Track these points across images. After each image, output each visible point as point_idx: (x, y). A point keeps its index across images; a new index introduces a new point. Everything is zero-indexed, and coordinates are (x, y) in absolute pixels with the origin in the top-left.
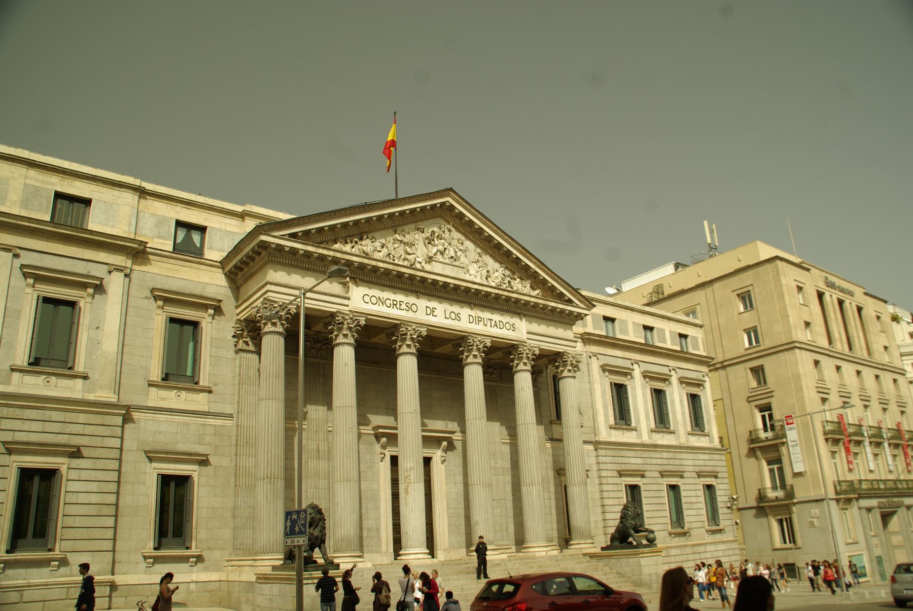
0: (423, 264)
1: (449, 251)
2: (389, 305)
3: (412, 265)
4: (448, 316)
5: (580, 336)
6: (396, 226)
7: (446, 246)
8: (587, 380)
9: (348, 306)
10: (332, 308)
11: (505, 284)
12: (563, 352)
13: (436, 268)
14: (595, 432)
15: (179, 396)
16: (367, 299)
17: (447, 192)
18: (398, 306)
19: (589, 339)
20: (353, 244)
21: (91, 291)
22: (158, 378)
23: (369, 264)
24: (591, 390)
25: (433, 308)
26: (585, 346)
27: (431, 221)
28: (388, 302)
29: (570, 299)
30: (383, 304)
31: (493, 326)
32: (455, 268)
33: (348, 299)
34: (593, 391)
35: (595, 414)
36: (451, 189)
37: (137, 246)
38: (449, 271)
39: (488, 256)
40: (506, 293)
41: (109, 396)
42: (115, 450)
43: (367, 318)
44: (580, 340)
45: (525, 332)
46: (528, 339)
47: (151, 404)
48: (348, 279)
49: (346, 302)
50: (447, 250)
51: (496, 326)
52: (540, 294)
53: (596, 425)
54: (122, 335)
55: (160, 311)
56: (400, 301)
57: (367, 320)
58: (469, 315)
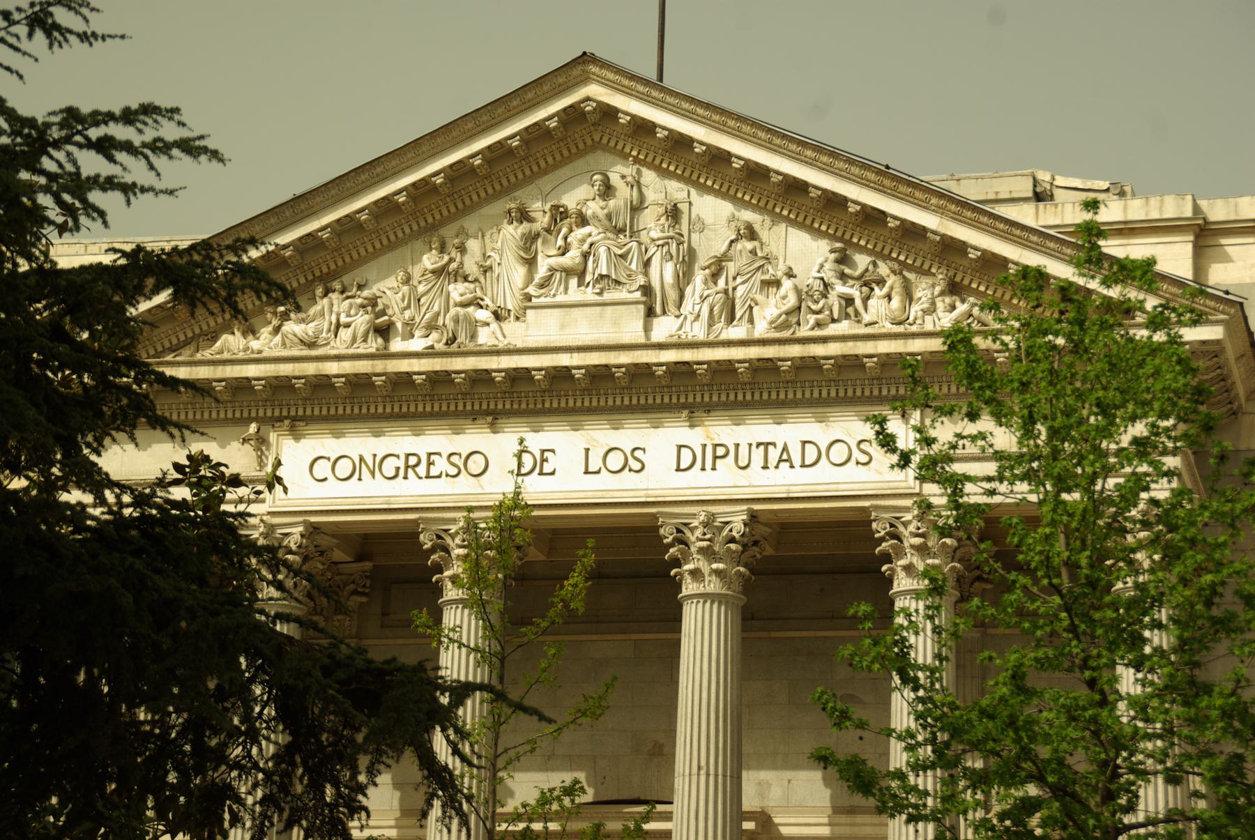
0: (494, 326)
1: (596, 261)
2: (392, 474)
3: (453, 339)
6: (432, 228)
7: (586, 247)
17: (576, 72)
18: (422, 470)
23: (297, 373)
25: (543, 451)
27: (564, 172)
28: (389, 467)
30: (373, 474)
31: (773, 461)
32: (609, 309)
36: (585, 58)
39: (784, 225)
50: (591, 259)
51: (789, 460)
56: (430, 454)
58: (680, 447)
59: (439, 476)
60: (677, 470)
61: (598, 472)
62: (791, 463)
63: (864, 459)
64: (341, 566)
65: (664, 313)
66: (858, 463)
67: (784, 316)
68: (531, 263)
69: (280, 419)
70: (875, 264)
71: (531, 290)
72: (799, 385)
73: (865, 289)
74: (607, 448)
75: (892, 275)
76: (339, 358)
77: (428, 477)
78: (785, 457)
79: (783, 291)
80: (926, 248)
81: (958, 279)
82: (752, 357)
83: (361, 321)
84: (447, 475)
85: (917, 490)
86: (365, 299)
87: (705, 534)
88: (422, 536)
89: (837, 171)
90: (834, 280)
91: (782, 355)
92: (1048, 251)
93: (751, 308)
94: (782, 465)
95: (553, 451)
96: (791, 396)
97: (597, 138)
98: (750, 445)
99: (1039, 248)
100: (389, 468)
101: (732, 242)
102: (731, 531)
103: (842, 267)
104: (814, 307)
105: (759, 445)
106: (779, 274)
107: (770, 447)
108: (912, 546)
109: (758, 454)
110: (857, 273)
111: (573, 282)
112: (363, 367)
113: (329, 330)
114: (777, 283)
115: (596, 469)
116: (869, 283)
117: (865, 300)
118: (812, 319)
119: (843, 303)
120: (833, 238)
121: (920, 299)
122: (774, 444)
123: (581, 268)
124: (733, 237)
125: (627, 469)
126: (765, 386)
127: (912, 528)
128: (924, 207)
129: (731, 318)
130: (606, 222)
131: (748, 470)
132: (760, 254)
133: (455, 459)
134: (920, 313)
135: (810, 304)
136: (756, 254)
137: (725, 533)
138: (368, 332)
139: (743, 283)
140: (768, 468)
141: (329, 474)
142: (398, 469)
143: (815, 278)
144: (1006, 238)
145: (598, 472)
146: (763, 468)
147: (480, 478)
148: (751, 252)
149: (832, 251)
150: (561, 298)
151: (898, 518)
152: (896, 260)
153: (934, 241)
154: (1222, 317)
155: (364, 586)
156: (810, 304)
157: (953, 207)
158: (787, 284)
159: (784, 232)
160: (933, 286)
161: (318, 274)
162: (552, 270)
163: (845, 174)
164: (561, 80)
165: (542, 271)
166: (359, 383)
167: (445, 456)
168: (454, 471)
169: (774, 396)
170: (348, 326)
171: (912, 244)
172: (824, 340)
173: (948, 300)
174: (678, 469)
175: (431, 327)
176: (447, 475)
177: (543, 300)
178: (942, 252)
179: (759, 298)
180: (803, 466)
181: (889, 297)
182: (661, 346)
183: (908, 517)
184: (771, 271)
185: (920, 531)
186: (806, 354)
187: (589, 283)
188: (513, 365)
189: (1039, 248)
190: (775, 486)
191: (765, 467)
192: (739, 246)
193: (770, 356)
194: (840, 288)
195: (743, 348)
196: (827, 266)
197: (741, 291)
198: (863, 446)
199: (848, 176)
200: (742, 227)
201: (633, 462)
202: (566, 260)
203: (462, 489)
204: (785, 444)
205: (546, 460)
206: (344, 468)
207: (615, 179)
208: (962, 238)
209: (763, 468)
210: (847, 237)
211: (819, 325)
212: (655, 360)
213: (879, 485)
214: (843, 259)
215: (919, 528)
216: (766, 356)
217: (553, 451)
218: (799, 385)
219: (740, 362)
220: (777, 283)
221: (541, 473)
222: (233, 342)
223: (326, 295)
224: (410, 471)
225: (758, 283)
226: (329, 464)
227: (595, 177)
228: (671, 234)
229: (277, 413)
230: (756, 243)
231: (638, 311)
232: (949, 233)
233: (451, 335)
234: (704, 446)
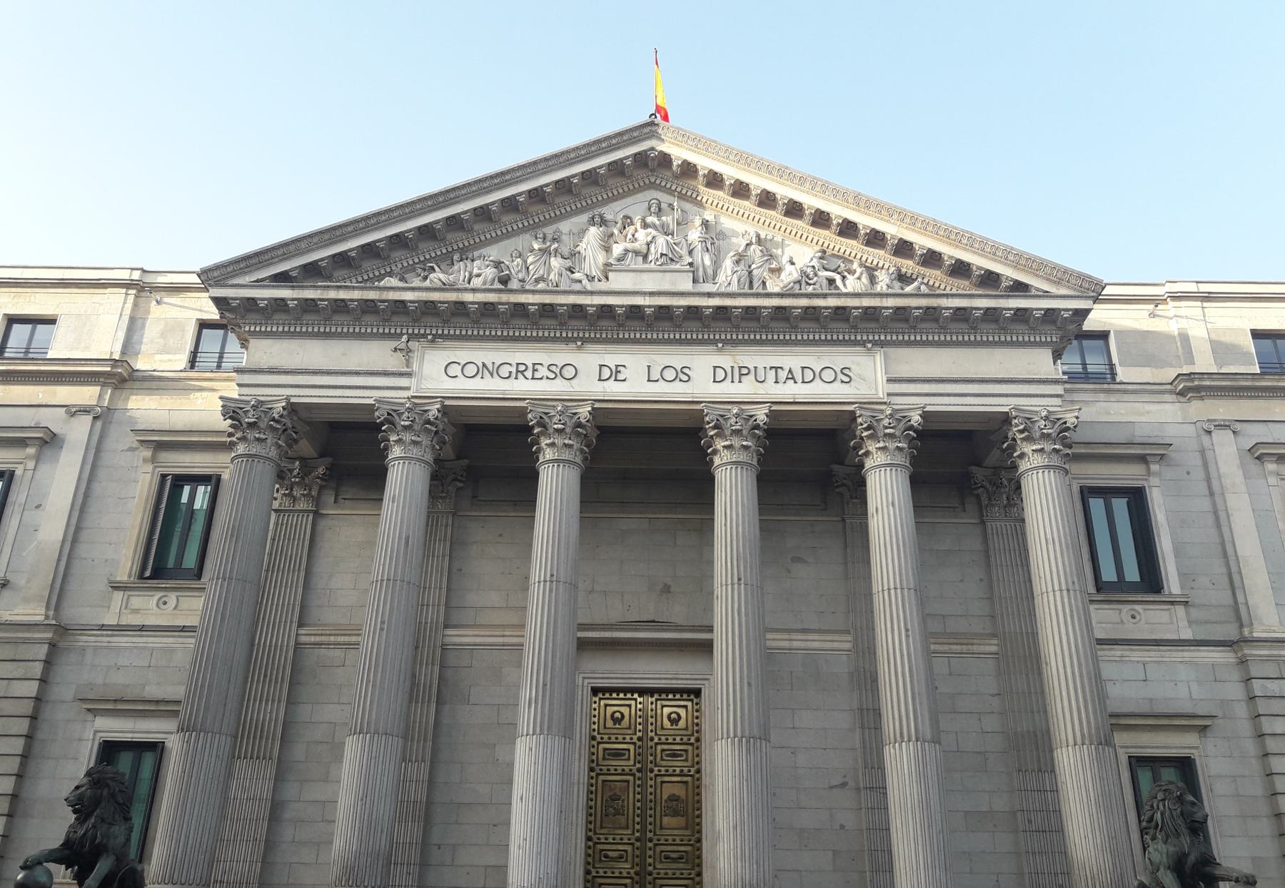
0: (585, 282)
2: (507, 376)
4: (656, 375)
5: (1169, 387)
6: (536, 226)
7: (649, 239)
8: (1203, 488)
9: (408, 389)
10: (367, 397)
13: (619, 281)
14: (1238, 614)
15: (165, 603)
16: (455, 370)
17: (646, 130)
18: (529, 374)
19: (1197, 389)
20: (426, 273)
21: (31, 451)
22: (130, 576)
23: (442, 299)
24: (1216, 513)
25: (617, 366)
28: (504, 371)
30: (492, 375)
33: (409, 375)
34: (1222, 515)
35: (1234, 569)
37: (109, 369)
38: (650, 282)
41: (36, 613)
42: (26, 701)
43: (444, 406)
45: (881, 378)
46: (889, 395)
47: (111, 620)
48: (405, 338)
49: (403, 382)
51: (793, 378)
52: (923, 287)
53: (1240, 599)
54: (76, 514)
55: (149, 468)
56: (534, 364)
57: (445, 410)
58: (715, 367)
59: (541, 379)
60: (714, 381)
61: (657, 381)
63: (847, 379)
64: (445, 463)
65: (704, 282)
66: (842, 382)
68: (608, 249)
69: (425, 336)
71: (611, 261)
74: (663, 366)
76: (474, 290)
77: (533, 378)
78: (790, 376)
83: (490, 272)
84: (547, 378)
86: (491, 261)
87: (736, 423)
88: (530, 416)
91: (795, 305)
95: (624, 366)
97: (653, 180)
100: (504, 371)
102: (756, 420)
104: (811, 282)
105: (771, 368)
107: (779, 370)
108: (886, 435)
110: (833, 268)
111: (641, 259)
112: (492, 297)
113: (464, 281)
114: (778, 271)
115: (656, 379)
123: (645, 251)
125: (678, 379)
127: (886, 422)
129: (751, 287)
130: (660, 229)
131: (764, 384)
133: (551, 368)
135: (807, 280)
137: (750, 423)
138: (494, 280)
140: (778, 382)
141: (459, 374)
142: (510, 372)
143: (808, 266)
145: (657, 381)
147: (571, 381)
150: (633, 266)
151: (874, 417)
155: (461, 476)
156: (807, 280)
158: (789, 268)
161: (455, 248)
162: (627, 251)
164: (635, 134)
165: (617, 249)
166: (488, 309)
167: (546, 365)
168: (553, 376)
170: (478, 275)
172: (825, 296)
174: (714, 381)
175: (537, 281)
176: (547, 378)
177: (619, 267)
180: (803, 382)
181: (859, 278)
182: (709, 295)
185: (892, 425)
187: (651, 261)
188: (603, 303)
191: (776, 382)
193: (787, 305)
201: (683, 375)
202: (636, 246)
203: (557, 387)
205: (619, 372)
206: (471, 370)
207: (664, 206)
211: (814, 289)
212: (705, 304)
217: (624, 366)
221: (616, 380)
222: (393, 282)
223: (461, 260)
224: (519, 374)
226: (460, 367)
227: (652, 202)
228: (707, 236)
229: (422, 331)
231: (688, 277)
233: (555, 284)
234: (732, 367)
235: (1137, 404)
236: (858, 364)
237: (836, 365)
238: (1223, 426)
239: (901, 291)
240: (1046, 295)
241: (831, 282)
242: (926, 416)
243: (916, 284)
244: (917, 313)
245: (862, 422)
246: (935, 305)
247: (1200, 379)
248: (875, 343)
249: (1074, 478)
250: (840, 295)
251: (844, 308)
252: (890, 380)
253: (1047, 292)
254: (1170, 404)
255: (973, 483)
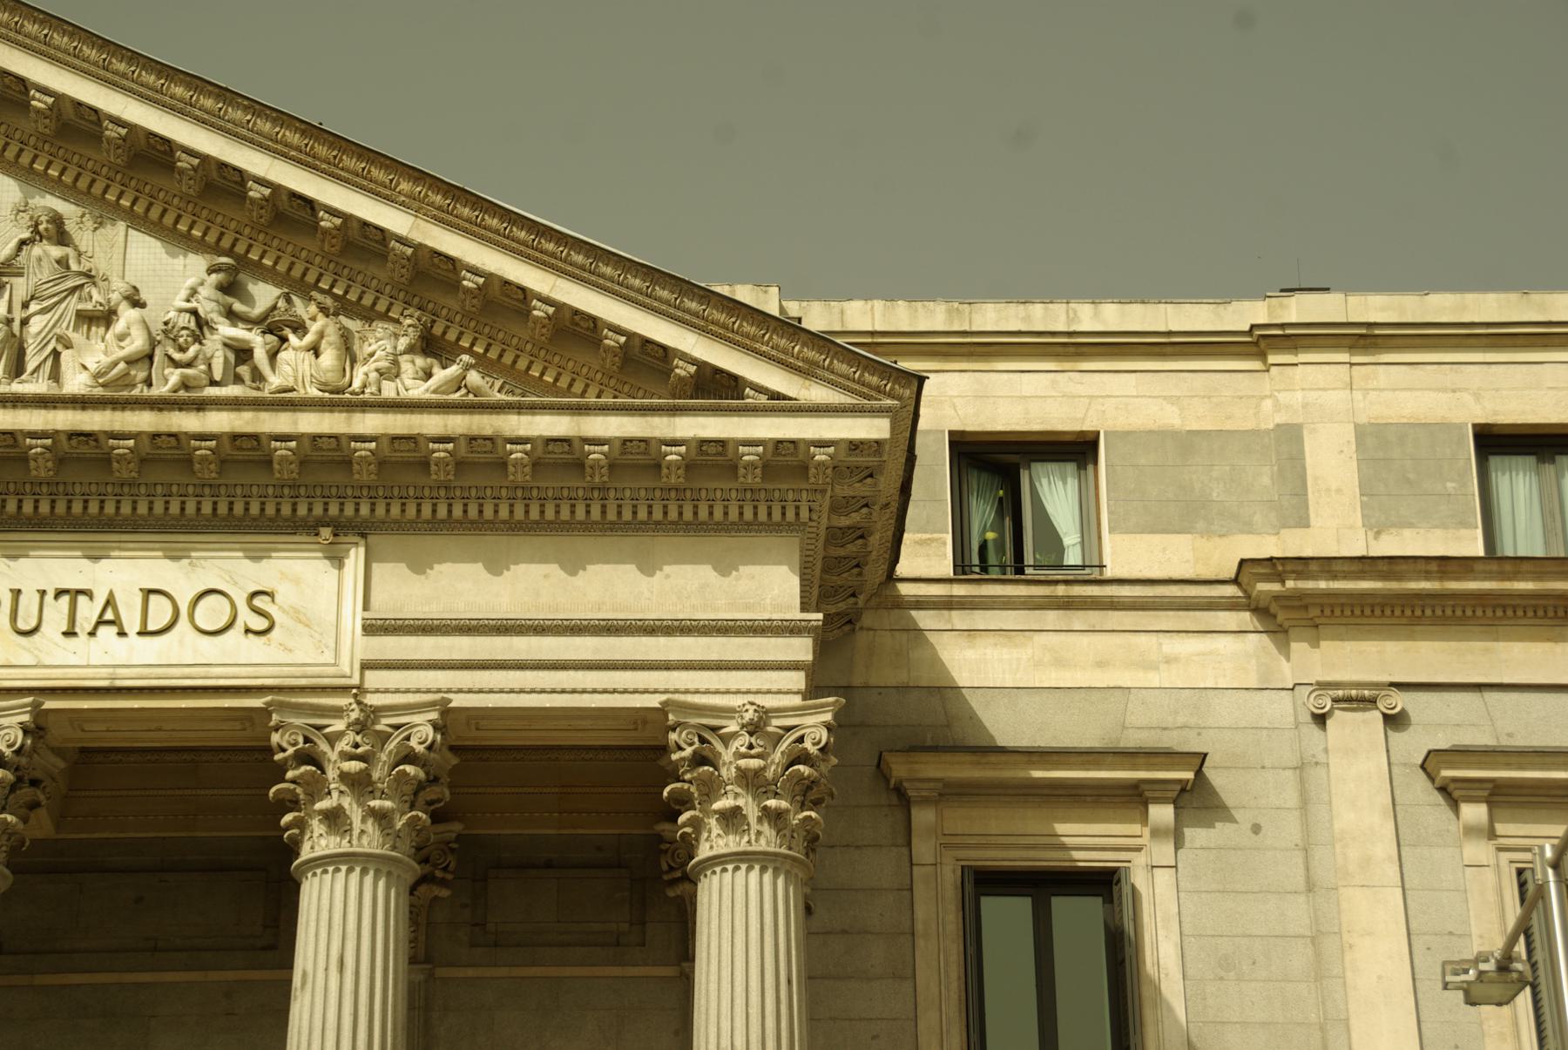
11: (177, 364)
12: (663, 710)
19: (1299, 602)
26: (1284, 649)
29: (702, 365)
39: (121, 226)
40: (144, 421)
44: (1245, 619)
45: (353, 618)
46: (367, 666)
52: (474, 377)
62: (121, 626)
63: (261, 624)
66: (248, 631)
67: (122, 365)
70: (289, 301)
72: (143, 490)
73: (270, 338)
75: (320, 314)
78: (109, 616)
79: (119, 326)
80: (383, 275)
81: (438, 330)
82: (59, 427)
85: (356, 681)
89: (230, 126)
90: (215, 316)
92: (601, 281)
93: (56, 354)
94: (102, 630)
96: (126, 509)
98: (43, 593)
99: (586, 275)
101: (23, 243)
103: (230, 300)
104: (177, 356)
105: (60, 593)
106: (115, 297)
107: (82, 599)
108: (344, 777)
109: (57, 612)
110: (258, 310)
114: (106, 317)
116: (277, 328)
117: (273, 356)
118: (175, 376)
119: (232, 357)
120: (216, 249)
121: (372, 355)
122: (87, 593)
124: (26, 235)
126: (78, 489)
127: (343, 745)
128: (386, 198)
131: (36, 637)
132: (74, 267)
134: (374, 375)
136: (68, 268)
139: (43, 311)
140: (74, 634)
143: (181, 311)
144: (528, 257)
146: (64, 634)
148: (58, 262)
149: (210, 271)
151: (319, 728)
152: (329, 292)
153: (403, 256)
154: (889, 402)
156: (171, 351)
157: (438, 199)
158: (127, 315)
159: (122, 239)
160: (396, 336)
163: (244, 132)
169: (93, 508)
171: (358, 266)
172: (201, 406)
173: (420, 361)
178: (411, 281)
179: (76, 337)
181: (315, 350)
183: (338, 725)
184: (96, 296)
185: (359, 750)
186: (163, 428)
189: (586, 275)
190: (88, 666)
191: (70, 633)
192: (37, 250)
193: (96, 428)
194: (226, 330)
195: (43, 412)
196: (204, 292)
197: (36, 324)
198: (257, 602)
199: (250, 135)
200: (43, 218)
204: (111, 594)
208: (452, 252)
209: (65, 634)
210: (240, 248)
211: (185, 385)
213: (286, 670)
214: (229, 288)
215: (356, 746)
216: (87, 428)
218: (143, 490)
219: (34, 435)
220: (106, 317)
225: (70, 316)
230: (69, 251)
232: (430, 243)
235: (1143, 638)
236: (297, 581)
237: (236, 583)
238: (1357, 698)
239: (419, 391)
240: (779, 404)
241: (243, 354)
242: (448, 719)
243: (454, 370)
244: (440, 452)
245: (285, 745)
246: (488, 432)
247: (1300, 575)
248: (341, 528)
249: (946, 846)
250: (235, 404)
251: (255, 437)
252: (371, 629)
253: (785, 398)
254: (1230, 638)
255: (665, 867)
